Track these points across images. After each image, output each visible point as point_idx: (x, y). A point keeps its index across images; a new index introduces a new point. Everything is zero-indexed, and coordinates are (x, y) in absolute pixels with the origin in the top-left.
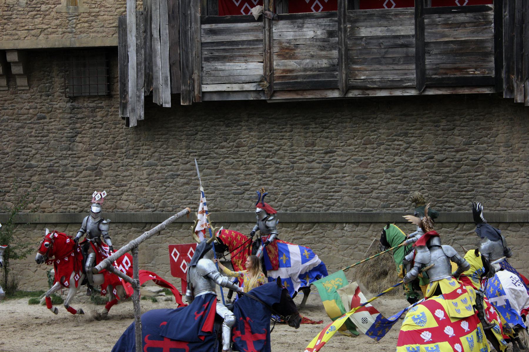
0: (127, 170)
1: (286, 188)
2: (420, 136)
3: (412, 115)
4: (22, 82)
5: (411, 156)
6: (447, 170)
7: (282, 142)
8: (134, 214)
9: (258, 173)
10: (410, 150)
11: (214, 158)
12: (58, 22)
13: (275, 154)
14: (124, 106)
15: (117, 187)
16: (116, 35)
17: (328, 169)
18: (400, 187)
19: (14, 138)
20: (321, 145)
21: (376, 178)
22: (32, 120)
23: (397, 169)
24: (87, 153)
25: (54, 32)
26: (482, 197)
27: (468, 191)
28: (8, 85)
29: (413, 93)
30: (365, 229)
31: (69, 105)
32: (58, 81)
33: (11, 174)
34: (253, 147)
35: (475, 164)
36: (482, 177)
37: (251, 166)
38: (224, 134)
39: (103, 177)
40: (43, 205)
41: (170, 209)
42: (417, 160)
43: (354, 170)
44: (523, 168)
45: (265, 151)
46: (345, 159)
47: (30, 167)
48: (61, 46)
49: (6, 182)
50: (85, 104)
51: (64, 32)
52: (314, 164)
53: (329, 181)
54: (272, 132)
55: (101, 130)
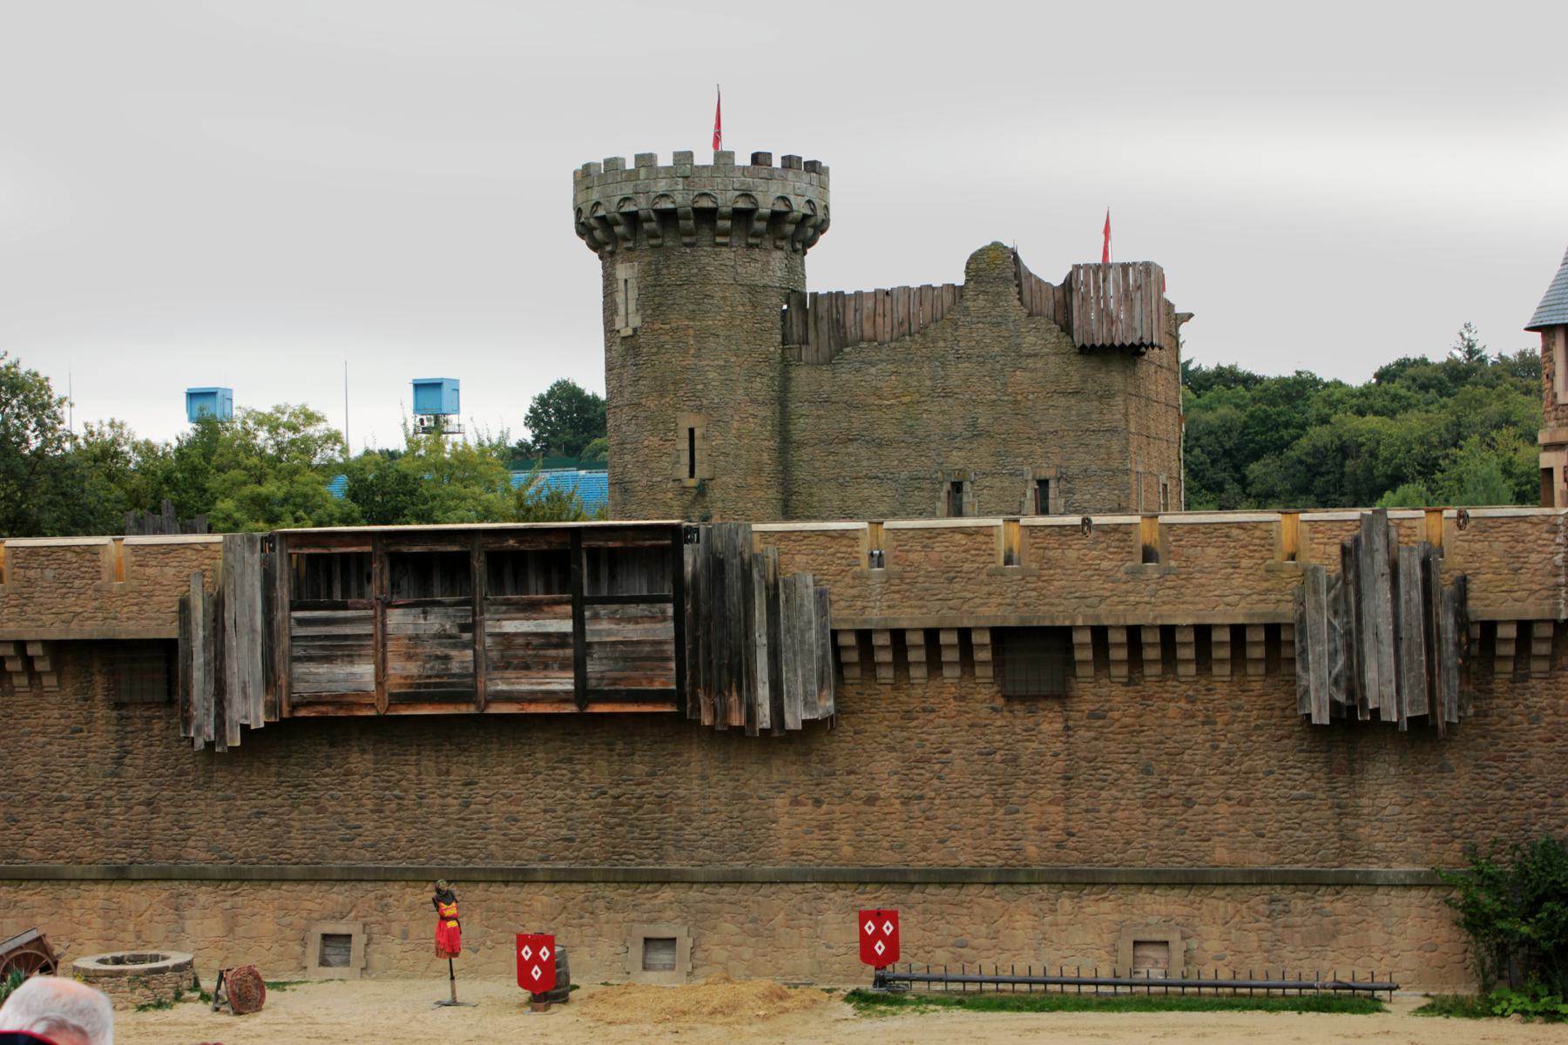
0: (195, 805)
1: (411, 832)
2: (590, 763)
3: (577, 734)
4: (50, 681)
5: (577, 790)
6: (624, 809)
7: (406, 769)
8: (204, 868)
9: (373, 811)
10: (576, 782)
11: (314, 790)
12: (95, 604)
13: (397, 784)
14: (187, 722)
15: (181, 828)
16: (176, 623)
17: (468, 807)
18: (563, 832)
19: (39, 758)
20: (458, 773)
21: (531, 820)
22: (64, 734)
23: (558, 808)
24: (140, 781)
25: (91, 618)
26: (671, 848)
27: (653, 839)
28: (31, 685)
29: (571, 709)
30: (518, 890)
31: (114, 714)
32: (100, 682)
33: (34, 810)
34: (367, 775)
35: (662, 802)
36: (671, 820)
37: (364, 801)
38: (328, 757)
39: (162, 814)
40: (80, 852)
41: (255, 860)
42: (585, 795)
43: (503, 809)
44: (723, 808)
45: (383, 781)
46: (490, 793)
47: (61, 799)
48: (101, 638)
49: (28, 820)
50: (138, 713)
51: (105, 618)
52: (449, 800)
53: (468, 823)
54: (393, 755)
55: (159, 750)
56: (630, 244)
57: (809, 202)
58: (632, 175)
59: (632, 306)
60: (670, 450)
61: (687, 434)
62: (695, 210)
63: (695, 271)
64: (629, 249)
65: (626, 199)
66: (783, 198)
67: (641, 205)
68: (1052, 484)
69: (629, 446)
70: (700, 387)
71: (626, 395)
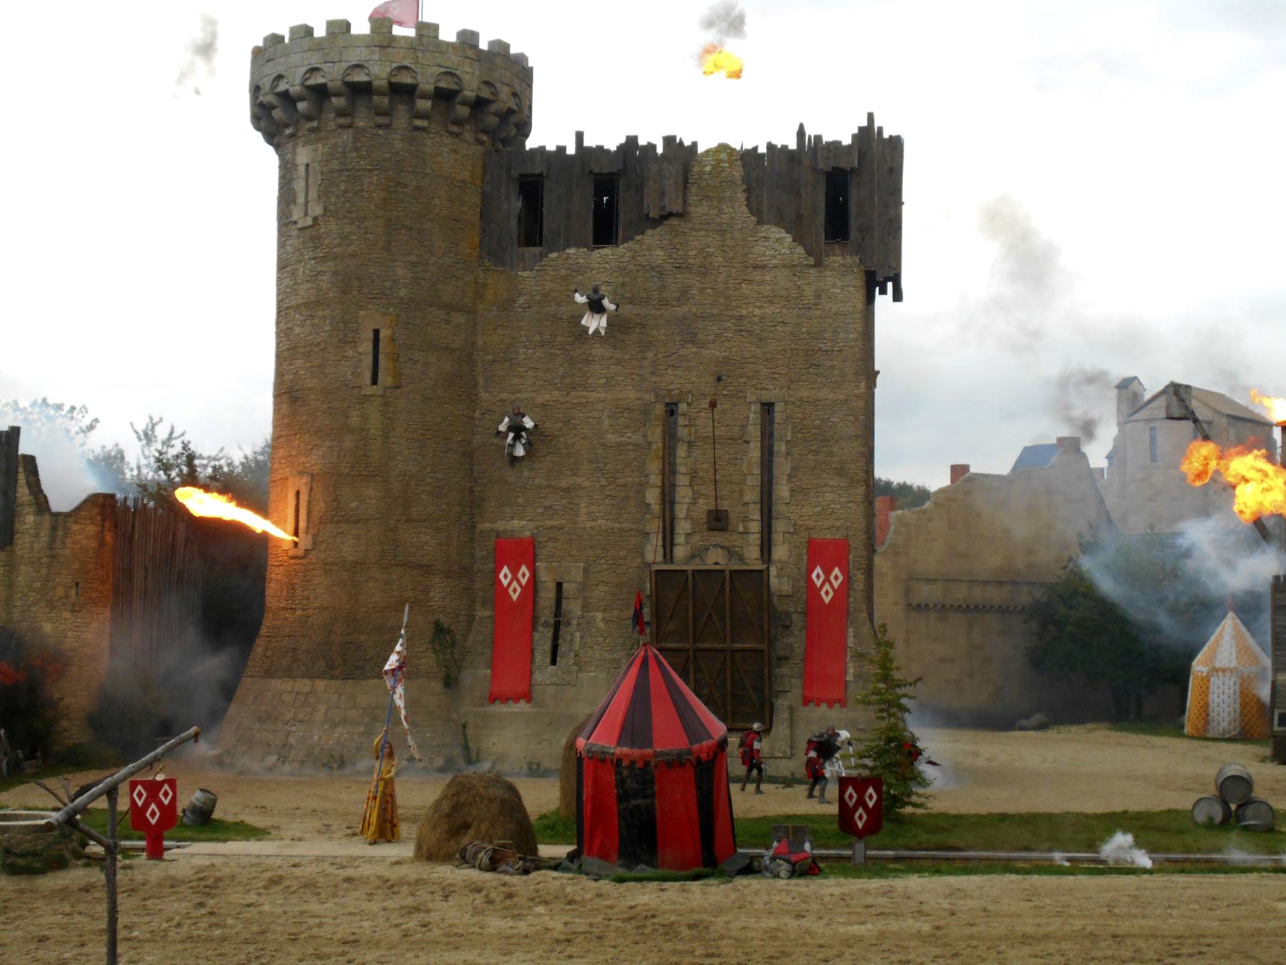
56: (315, 124)
57: (515, 95)
58: (319, 45)
59: (313, 194)
60: (350, 353)
61: (371, 335)
62: (391, 84)
63: (388, 155)
64: (312, 130)
65: (313, 70)
66: (487, 83)
67: (331, 75)
68: (777, 408)
69: (301, 350)
70: (388, 284)
71: (301, 293)
